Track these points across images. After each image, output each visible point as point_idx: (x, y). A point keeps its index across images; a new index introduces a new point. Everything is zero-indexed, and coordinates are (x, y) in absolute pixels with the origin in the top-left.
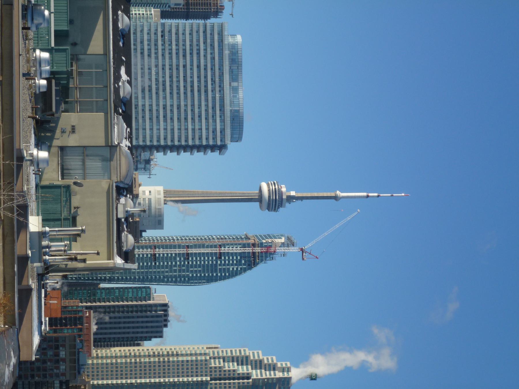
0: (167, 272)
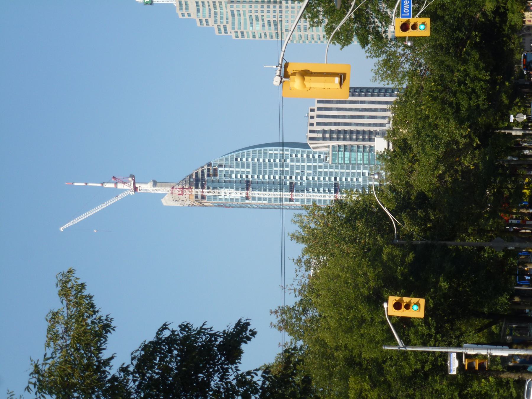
0: (320, 167)
